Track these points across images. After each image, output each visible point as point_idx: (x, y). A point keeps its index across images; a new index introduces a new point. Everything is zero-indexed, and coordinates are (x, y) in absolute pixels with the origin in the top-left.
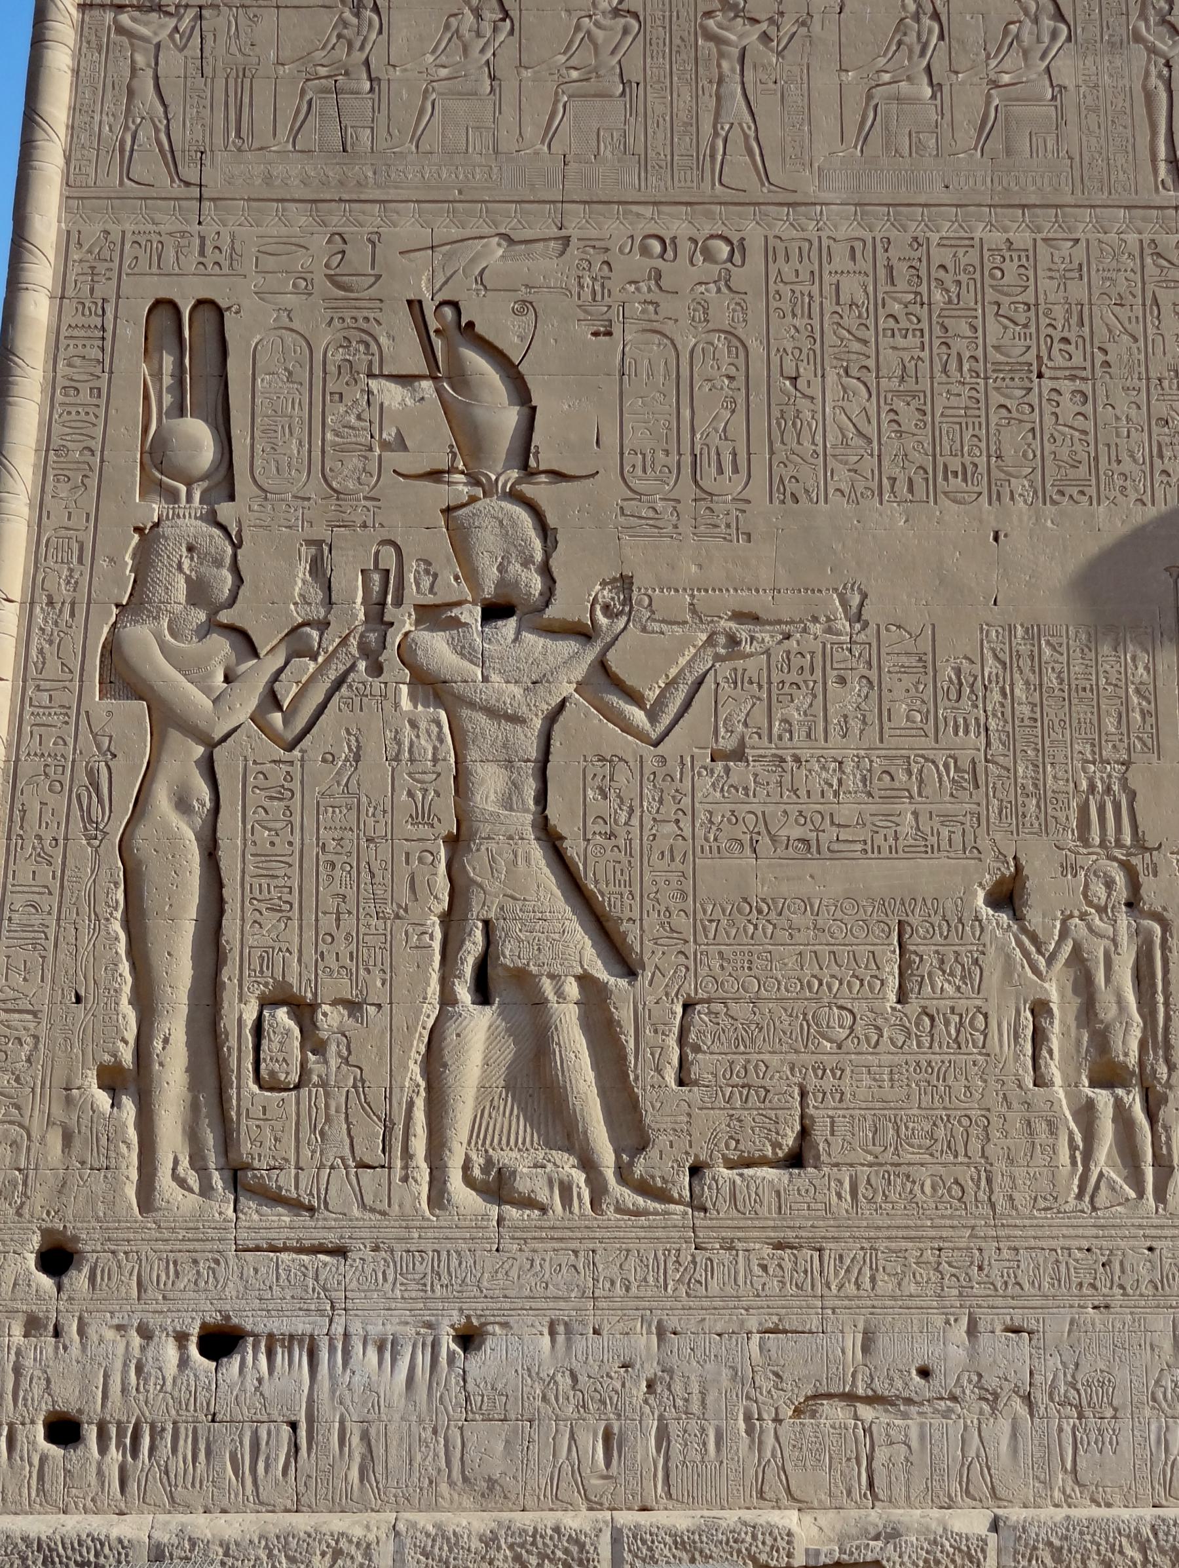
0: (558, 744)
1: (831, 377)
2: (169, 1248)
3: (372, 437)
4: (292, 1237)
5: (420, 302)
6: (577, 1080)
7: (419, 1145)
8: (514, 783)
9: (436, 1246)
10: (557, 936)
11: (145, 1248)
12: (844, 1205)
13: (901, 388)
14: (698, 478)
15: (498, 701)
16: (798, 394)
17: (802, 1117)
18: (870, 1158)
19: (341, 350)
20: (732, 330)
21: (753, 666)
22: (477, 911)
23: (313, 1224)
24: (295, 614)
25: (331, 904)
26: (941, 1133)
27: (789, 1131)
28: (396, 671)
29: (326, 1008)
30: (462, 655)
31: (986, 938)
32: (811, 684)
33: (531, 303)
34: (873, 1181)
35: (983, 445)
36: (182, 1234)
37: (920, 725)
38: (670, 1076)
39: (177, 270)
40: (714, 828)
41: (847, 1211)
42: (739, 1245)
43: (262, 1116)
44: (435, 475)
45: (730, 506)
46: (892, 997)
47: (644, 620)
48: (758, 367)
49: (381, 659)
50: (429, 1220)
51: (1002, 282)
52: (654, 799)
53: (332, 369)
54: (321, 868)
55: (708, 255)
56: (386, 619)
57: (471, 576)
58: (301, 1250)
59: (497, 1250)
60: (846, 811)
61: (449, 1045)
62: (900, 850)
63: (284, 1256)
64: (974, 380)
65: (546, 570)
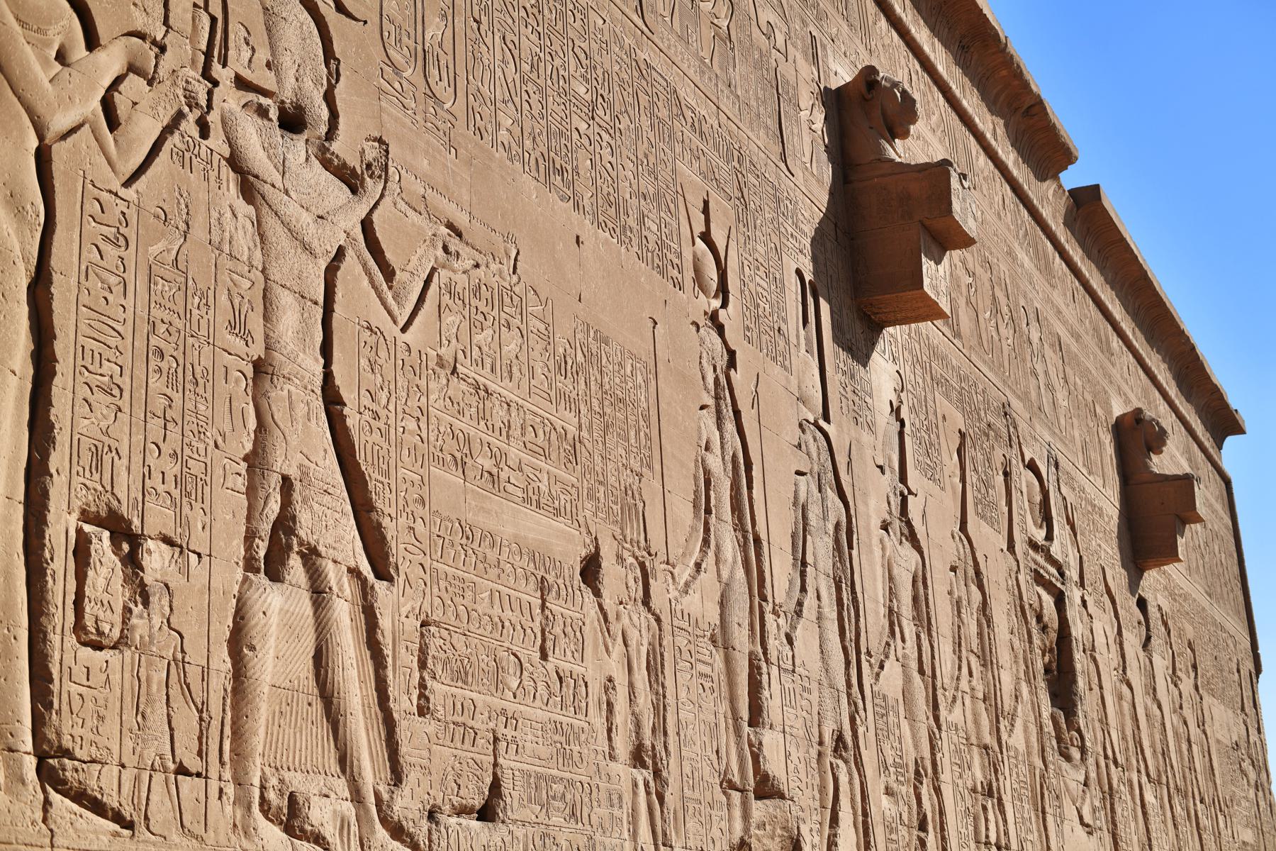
54: (150, 355)
61: (257, 624)
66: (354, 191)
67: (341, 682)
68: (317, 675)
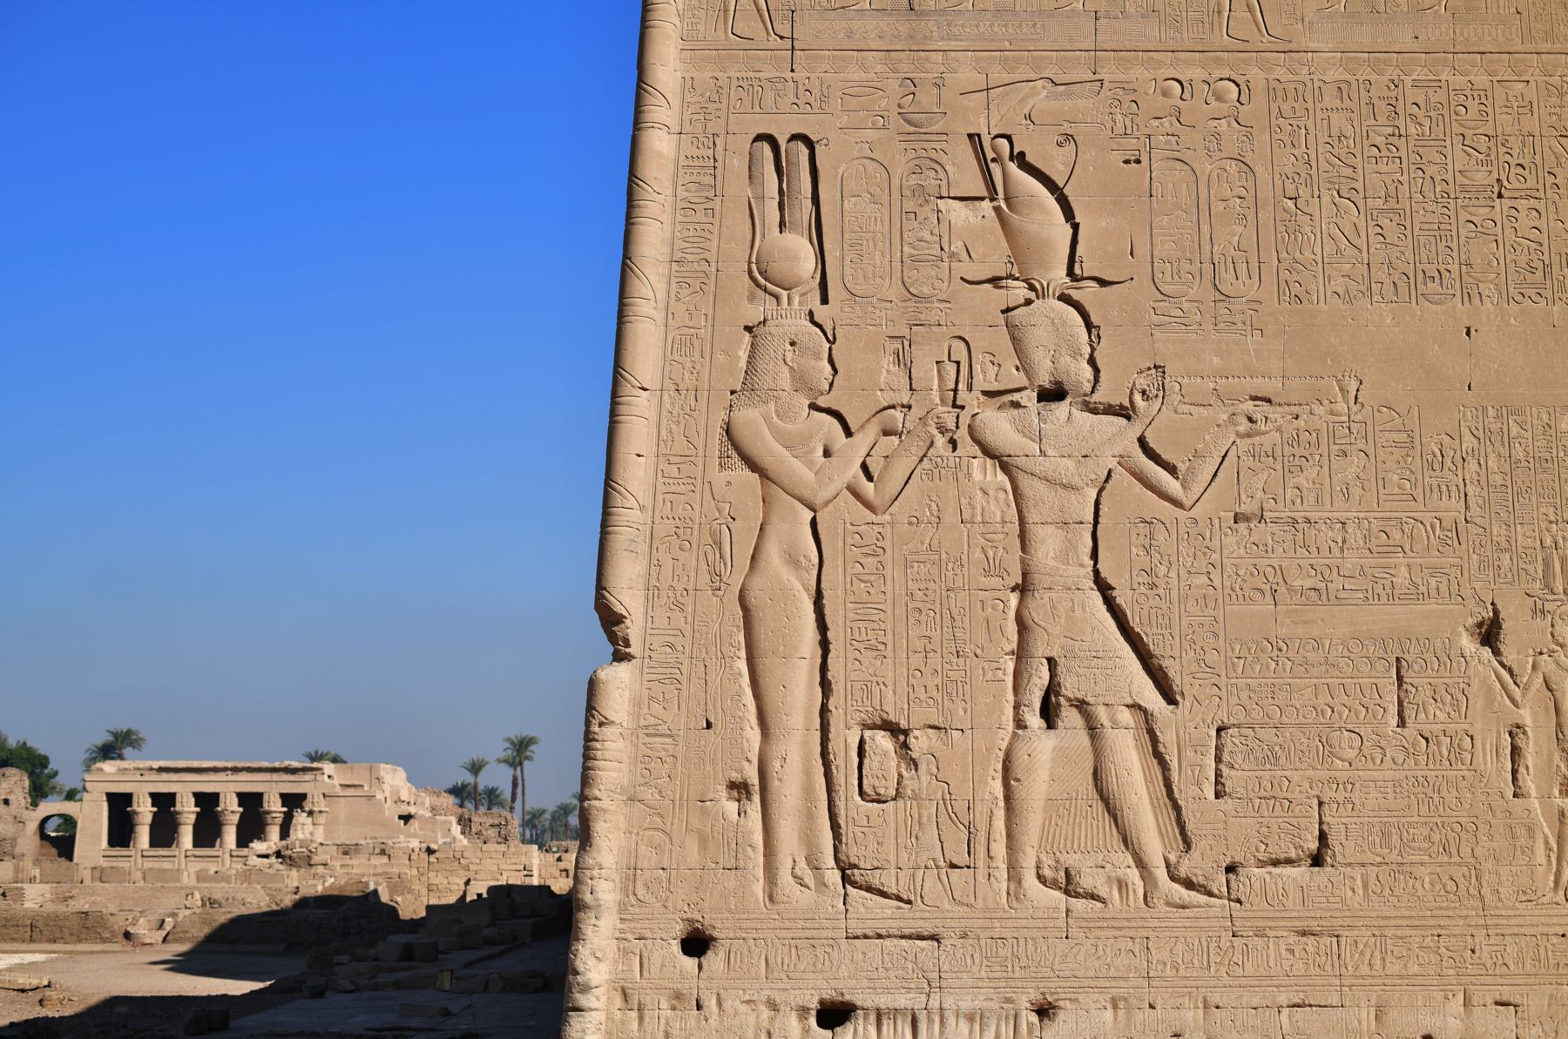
0: (1106, 509)
1: (1326, 199)
2: (791, 935)
3: (942, 249)
4: (893, 926)
5: (979, 136)
6: (1130, 794)
7: (1000, 848)
8: (1069, 541)
9: (1015, 935)
10: (1109, 672)
11: (770, 935)
12: (1357, 899)
13: (1385, 207)
14: (1217, 283)
15: (1054, 472)
16: (1299, 212)
17: (1321, 823)
18: (1379, 859)
19: (914, 176)
20: (1241, 158)
21: (1266, 442)
22: (1041, 649)
23: (911, 915)
24: (882, 399)
25: (919, 645)
26: (1436, 837)
27: (1309, 836)
28: (967, 447)
29: (916, 732)
30: (1025, 435)
31: (1471, 672)
32: (1318, 457)
33: (1071, 136)
34: (1380, 879)
35: (1455, 254)
36: (801, 924)
37: (1409, 491)
38: (1210, 792)
39: (775, 110)
40: (1239, 580)
41: (1360, 904)
42: (1270, 933)
43: (865, 824)
44: (994, 281)
45: (1245, 307)
46: (1394, 721)
47: (1176, 403)
48: (1266, 192)
49: (955, 437)
50: (1008, 912)
51: (1465, 118)
52: (1188, 554)
53: (907, 192)
55: (1219, 98)
56: (958, 403)
57: (1024, 366)
58: (902, 937)
59: (1067, 938)
60: (1350, 564)
62: (1396, 598)
63: (887, 942)
64: (1444, 200)
65: (1092, 361)
66: (1128, 418)
67: (1116, 788)
68: (1096, 786)
